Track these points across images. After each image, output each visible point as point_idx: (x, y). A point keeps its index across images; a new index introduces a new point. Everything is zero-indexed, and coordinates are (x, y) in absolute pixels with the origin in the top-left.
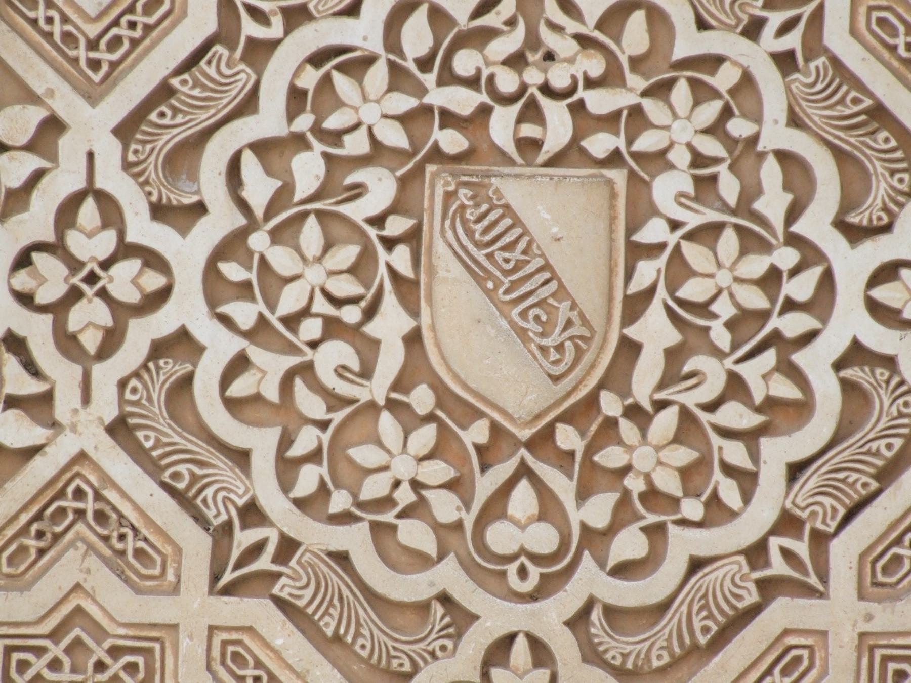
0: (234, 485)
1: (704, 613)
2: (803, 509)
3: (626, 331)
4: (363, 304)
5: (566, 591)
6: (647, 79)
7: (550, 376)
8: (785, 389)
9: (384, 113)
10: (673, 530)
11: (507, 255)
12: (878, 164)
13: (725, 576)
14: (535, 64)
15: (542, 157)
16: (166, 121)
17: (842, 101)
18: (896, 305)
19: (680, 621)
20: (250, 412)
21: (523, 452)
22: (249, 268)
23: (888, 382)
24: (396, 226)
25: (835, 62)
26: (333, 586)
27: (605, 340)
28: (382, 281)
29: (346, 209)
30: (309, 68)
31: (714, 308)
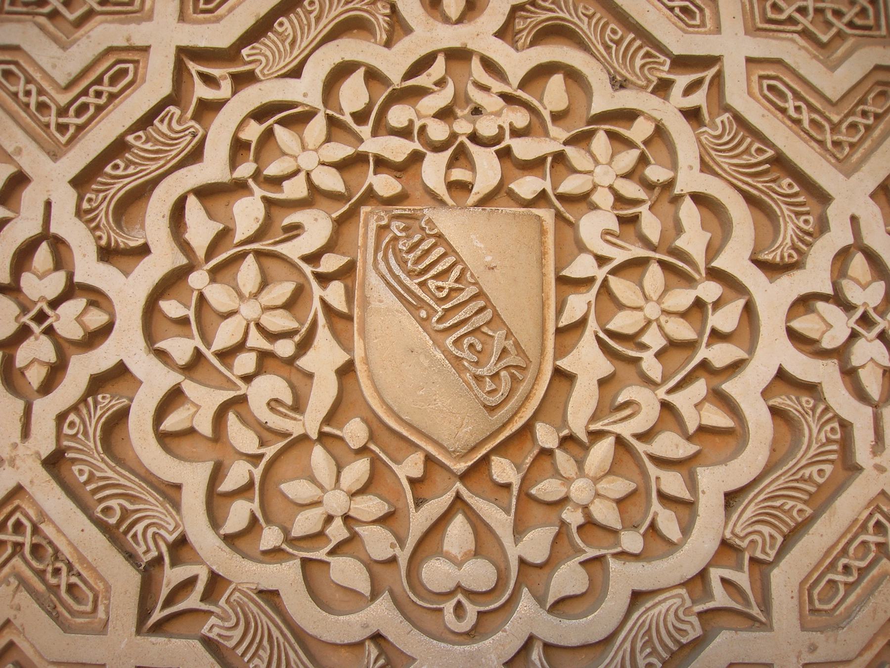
0: (165, 521)
1: (648, 650)
2: (742, 539)
3: (559, 363)
4: (297, 338)
5: (505, 631)
6: (568, 131)
7: (485, 406)
8: (717, 418)
9: (321, 160)
10: (614, 565)
11: (440, 284)
12: (783, 207)
13: (668, 610)
14: (464, 117)
15: (473, 198)
16: (119, 172)
17: (747, 151)
18: (815, 336)
19: (623, 658)
20: (185, 446)
21: (458, 485)
22: (187, 307)
23: (813, 409)
24: (330, 263)
25: (739, 119)
26: (262, 626)
27: (539, 371)
28: (316, 315)
29: (283, 249)
30: (253, 123)
31: (645, 339)
